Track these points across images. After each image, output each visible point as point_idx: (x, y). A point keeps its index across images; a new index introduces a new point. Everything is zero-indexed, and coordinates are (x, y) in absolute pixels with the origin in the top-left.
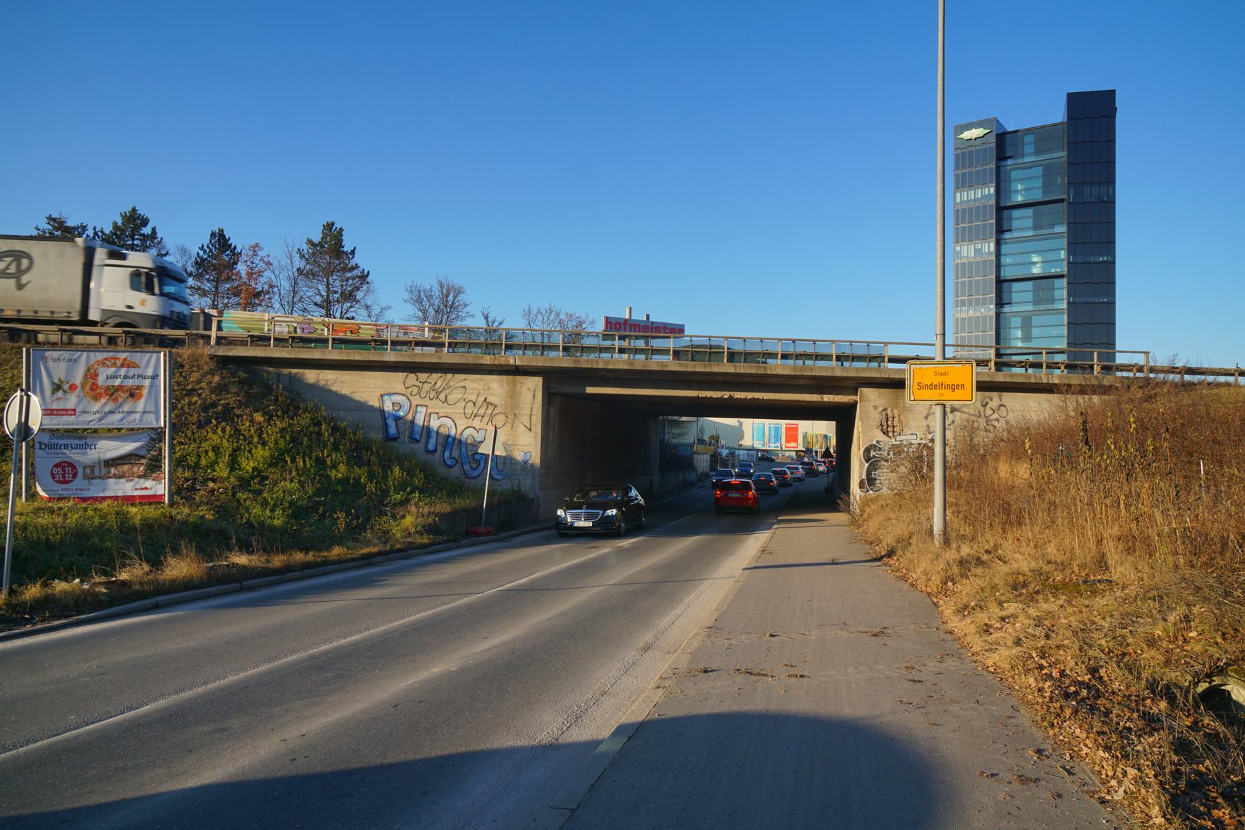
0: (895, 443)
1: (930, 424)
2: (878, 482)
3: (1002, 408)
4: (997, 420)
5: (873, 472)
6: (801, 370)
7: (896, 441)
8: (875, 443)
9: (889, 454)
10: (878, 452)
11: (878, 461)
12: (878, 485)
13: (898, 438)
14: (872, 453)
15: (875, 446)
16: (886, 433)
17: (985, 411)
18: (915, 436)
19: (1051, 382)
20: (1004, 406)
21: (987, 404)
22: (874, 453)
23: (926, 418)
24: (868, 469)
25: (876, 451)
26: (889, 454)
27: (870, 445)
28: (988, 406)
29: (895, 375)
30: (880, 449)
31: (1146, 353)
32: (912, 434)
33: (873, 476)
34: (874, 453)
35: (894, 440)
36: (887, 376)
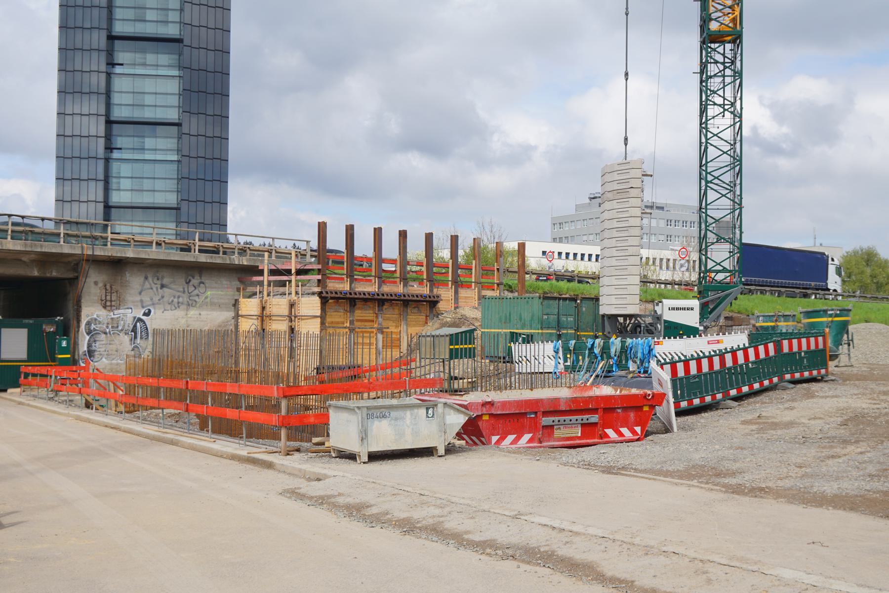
0: (113, 316)
1: (143, 299)
2: (98, 353)
3: (202, 285)
4: (198, 295)
5: (93, 345)
6: (32, 247)
7: (114, 315)
8: (95, 316)
9: (107, 327)
10: (98, 326)
11: (99, 333)
12: (98, 356)
13: (116, 312)
14: (93, 326)
15: (96, 320)
16: (105, 307)
17: (188, 288)
18: (130, 310)
19: (241, 263)
20: (203, 283)
21: (190, 281)
22: (94, 327)
23: (140, 293)
24: (89, 341)
25: (96, 324)
26: (107, 327)
27: (91, 319)
28: (191, 283)
29: (117, 253)
30: (100, 323)
31: (308, 242)
32: (128, 308)
33: (94, 348)
34: (94, 327)
35: (112, 313)
36: (110, 255)
